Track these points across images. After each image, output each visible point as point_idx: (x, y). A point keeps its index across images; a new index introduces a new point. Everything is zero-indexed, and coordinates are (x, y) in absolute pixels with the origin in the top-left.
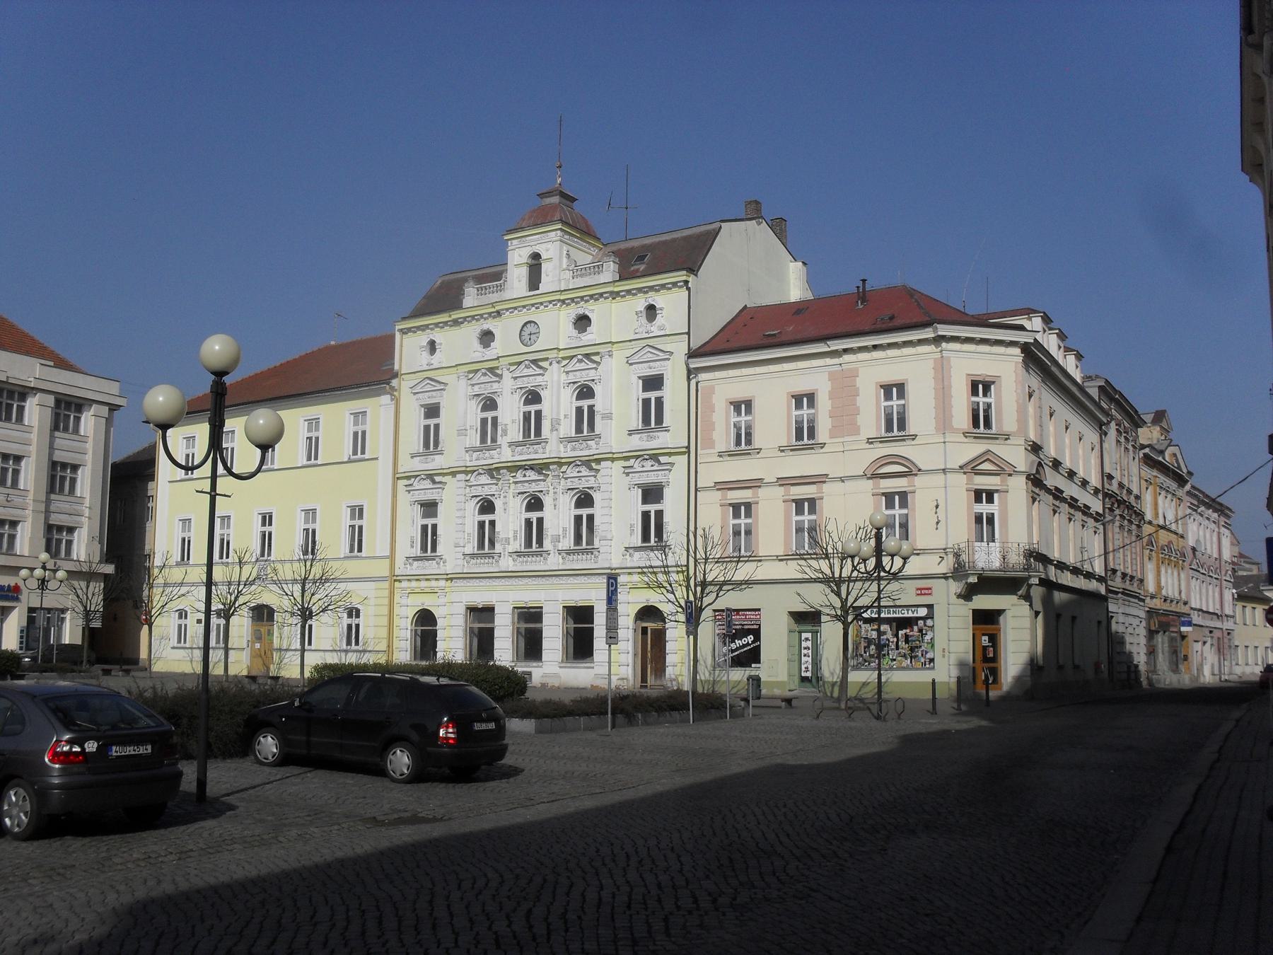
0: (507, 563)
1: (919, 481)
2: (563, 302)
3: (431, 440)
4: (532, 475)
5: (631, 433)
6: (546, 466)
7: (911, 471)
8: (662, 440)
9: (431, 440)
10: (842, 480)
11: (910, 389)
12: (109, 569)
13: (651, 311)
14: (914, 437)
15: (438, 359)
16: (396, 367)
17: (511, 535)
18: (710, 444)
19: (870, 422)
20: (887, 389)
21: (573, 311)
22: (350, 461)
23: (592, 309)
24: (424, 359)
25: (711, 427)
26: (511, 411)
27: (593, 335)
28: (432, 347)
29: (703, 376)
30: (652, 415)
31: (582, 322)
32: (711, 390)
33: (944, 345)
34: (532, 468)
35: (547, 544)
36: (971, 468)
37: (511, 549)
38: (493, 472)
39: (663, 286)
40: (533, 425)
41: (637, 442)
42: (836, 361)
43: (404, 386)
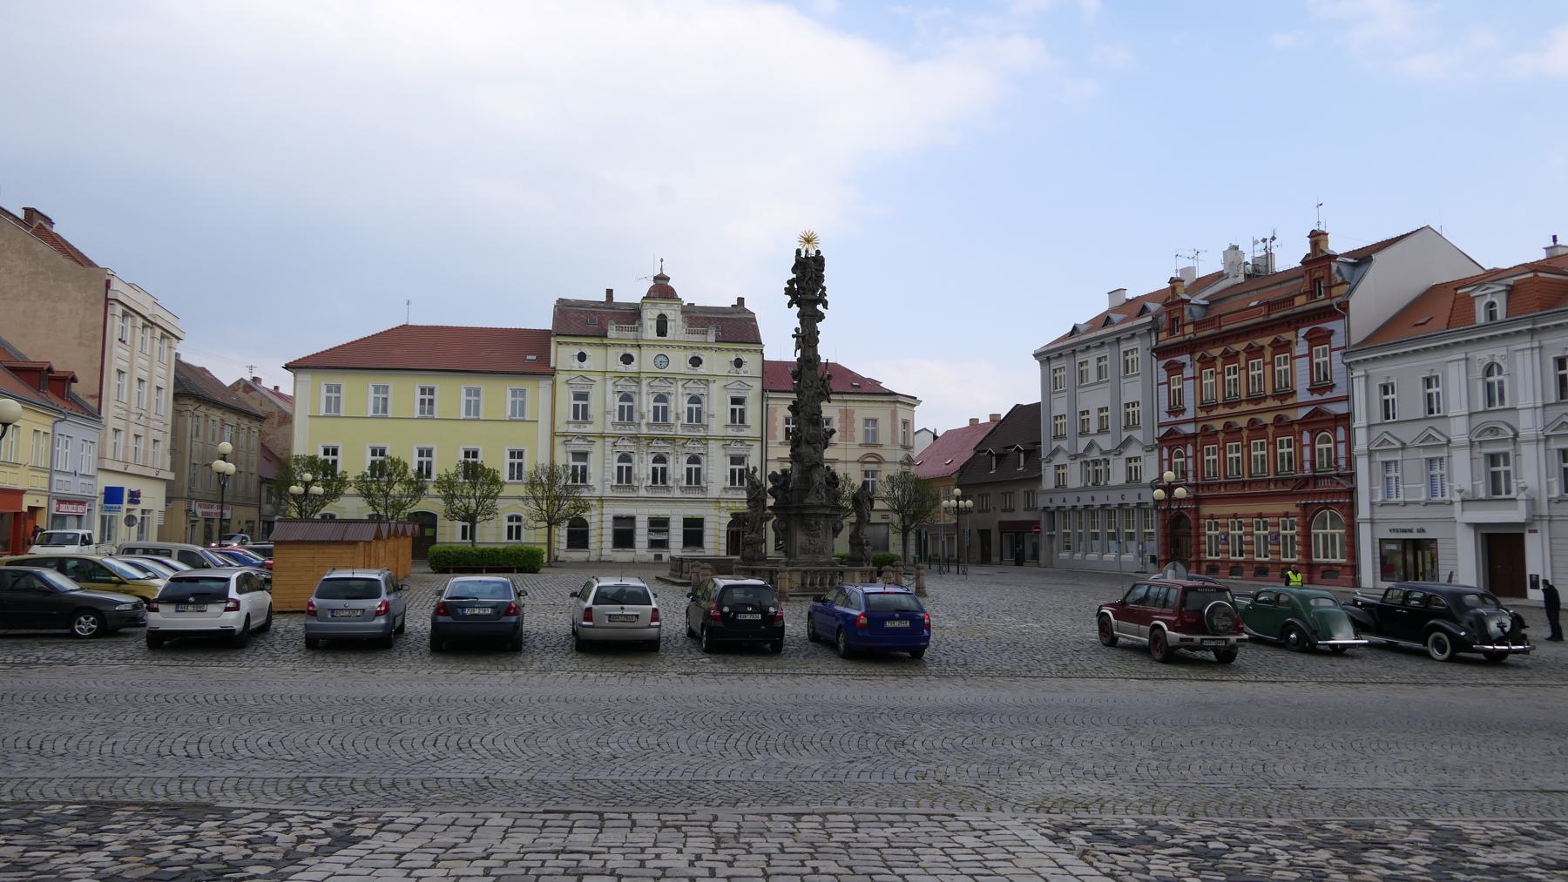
0: (643, 493)
1: (883, 466)
2: (685, 347)
3: (581, 414)
4: (661, 444)
5: (727, 426)
6: (674, 439)
7: (880, 461)
8: (745, 433)
9: (581, 414)
10: (846, 462)
11: (880, 422)
12: (171, 476)
13: (739, 363)
14: (881, 445)
15: (585, 365)
16: (552, 365)
17: (645, 476)
18: (775, 438)
19: (859, 437)
20: (867, 420)
21: (690, 354)
22: (511, 421)
23: (704, 356)
24: (576, 364)
25: (776, 428)
26: (646, 404)
27: (701, 370)
28: (582, 357)
29: (770, 402)
30: (738, 417)
31: (696, 362)
32: (775, 410)
33: (898, 405)
34: (663, 439)
35: (670, 483)
36: (862, 462)
37: (644, 484)
38: (636, 438)
39: (749, 350)
40: (661, 415)
41: (731, 432)
42: (844, 404)
43: (560, 378)
